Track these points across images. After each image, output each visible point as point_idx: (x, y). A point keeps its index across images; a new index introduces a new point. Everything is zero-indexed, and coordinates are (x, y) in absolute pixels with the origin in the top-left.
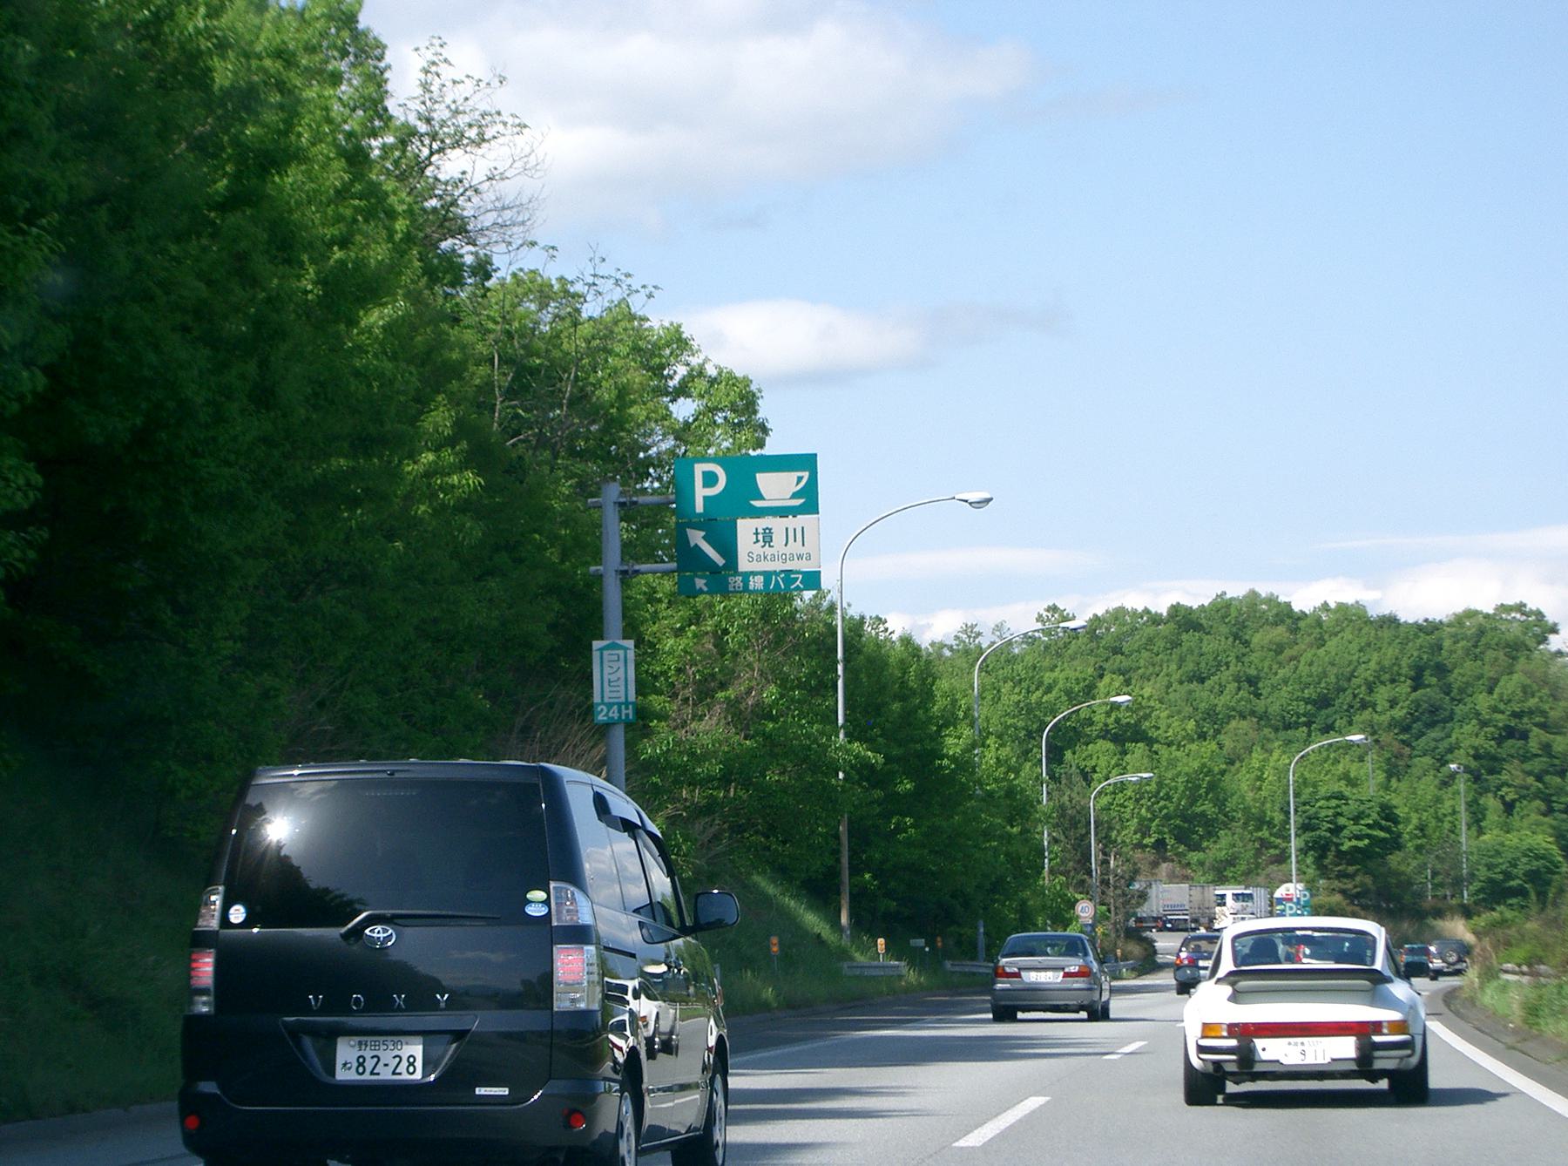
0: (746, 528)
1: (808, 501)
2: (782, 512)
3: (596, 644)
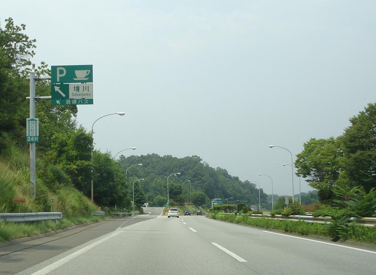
0: (72, 85)
1: (90, 78)
2: (82, 82)
3: (27, 119)
